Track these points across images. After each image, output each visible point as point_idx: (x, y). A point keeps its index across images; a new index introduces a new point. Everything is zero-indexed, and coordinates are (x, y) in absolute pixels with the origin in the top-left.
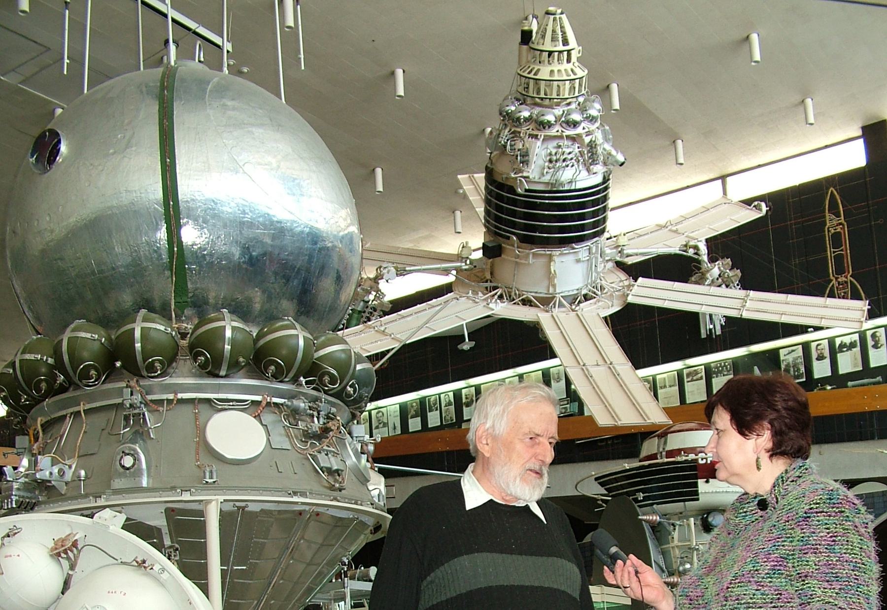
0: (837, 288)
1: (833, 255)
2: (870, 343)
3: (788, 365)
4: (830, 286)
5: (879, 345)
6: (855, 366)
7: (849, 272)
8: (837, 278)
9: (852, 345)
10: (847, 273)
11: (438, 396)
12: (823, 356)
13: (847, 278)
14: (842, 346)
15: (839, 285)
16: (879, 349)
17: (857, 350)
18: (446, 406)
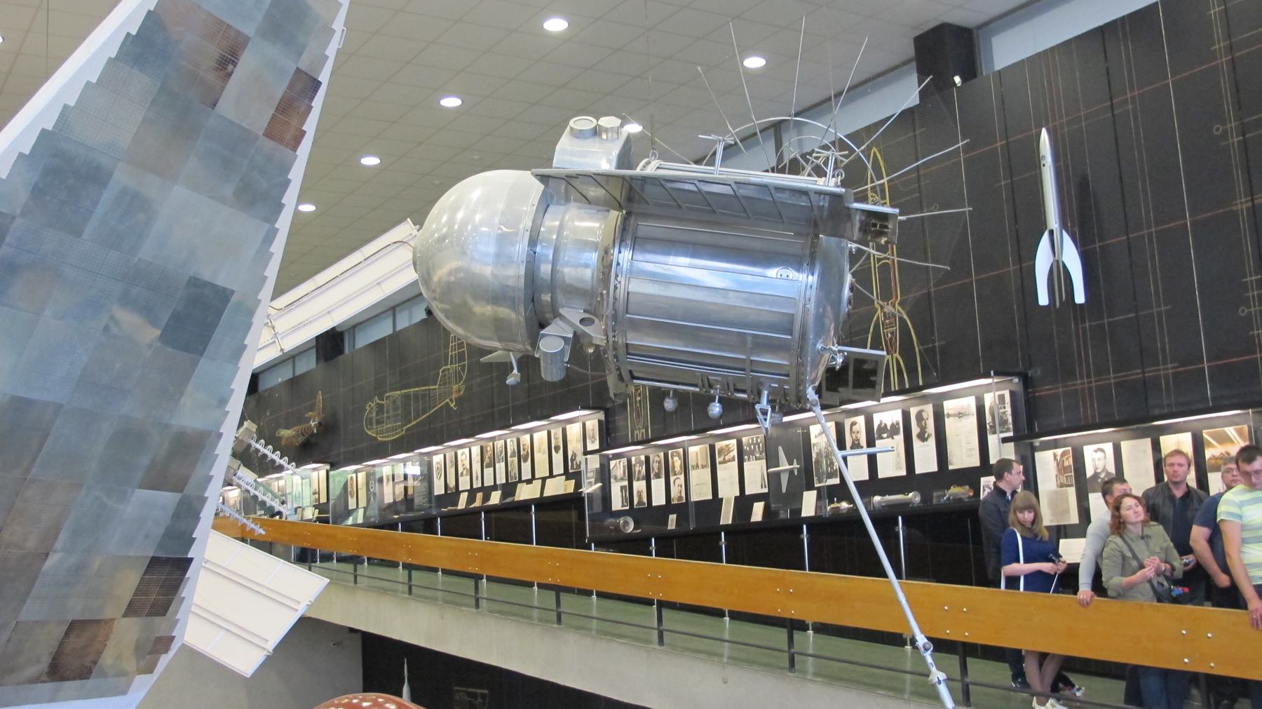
0: (883, 324)
1: (877, 266)
2: (915, 430)
3: (819, 454)
4: (875, 319)
5: (926, 435)
6: (899, 468)
7: (897, 298)
8: (882, 307)
9: (893, 431)
10: (894, 299)
11: (503, 441)
12: (859, 443)
13: (894, 307)
14: (883, 429)
15: (885, 320)
16: (925, 443)
17: (900, 438)
18: (511, 457)
